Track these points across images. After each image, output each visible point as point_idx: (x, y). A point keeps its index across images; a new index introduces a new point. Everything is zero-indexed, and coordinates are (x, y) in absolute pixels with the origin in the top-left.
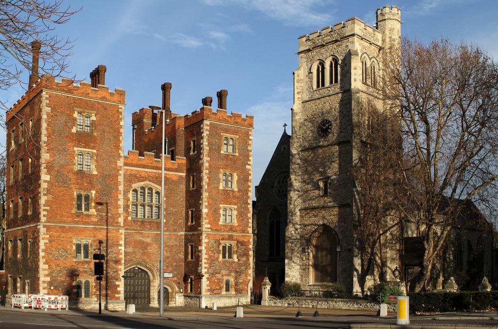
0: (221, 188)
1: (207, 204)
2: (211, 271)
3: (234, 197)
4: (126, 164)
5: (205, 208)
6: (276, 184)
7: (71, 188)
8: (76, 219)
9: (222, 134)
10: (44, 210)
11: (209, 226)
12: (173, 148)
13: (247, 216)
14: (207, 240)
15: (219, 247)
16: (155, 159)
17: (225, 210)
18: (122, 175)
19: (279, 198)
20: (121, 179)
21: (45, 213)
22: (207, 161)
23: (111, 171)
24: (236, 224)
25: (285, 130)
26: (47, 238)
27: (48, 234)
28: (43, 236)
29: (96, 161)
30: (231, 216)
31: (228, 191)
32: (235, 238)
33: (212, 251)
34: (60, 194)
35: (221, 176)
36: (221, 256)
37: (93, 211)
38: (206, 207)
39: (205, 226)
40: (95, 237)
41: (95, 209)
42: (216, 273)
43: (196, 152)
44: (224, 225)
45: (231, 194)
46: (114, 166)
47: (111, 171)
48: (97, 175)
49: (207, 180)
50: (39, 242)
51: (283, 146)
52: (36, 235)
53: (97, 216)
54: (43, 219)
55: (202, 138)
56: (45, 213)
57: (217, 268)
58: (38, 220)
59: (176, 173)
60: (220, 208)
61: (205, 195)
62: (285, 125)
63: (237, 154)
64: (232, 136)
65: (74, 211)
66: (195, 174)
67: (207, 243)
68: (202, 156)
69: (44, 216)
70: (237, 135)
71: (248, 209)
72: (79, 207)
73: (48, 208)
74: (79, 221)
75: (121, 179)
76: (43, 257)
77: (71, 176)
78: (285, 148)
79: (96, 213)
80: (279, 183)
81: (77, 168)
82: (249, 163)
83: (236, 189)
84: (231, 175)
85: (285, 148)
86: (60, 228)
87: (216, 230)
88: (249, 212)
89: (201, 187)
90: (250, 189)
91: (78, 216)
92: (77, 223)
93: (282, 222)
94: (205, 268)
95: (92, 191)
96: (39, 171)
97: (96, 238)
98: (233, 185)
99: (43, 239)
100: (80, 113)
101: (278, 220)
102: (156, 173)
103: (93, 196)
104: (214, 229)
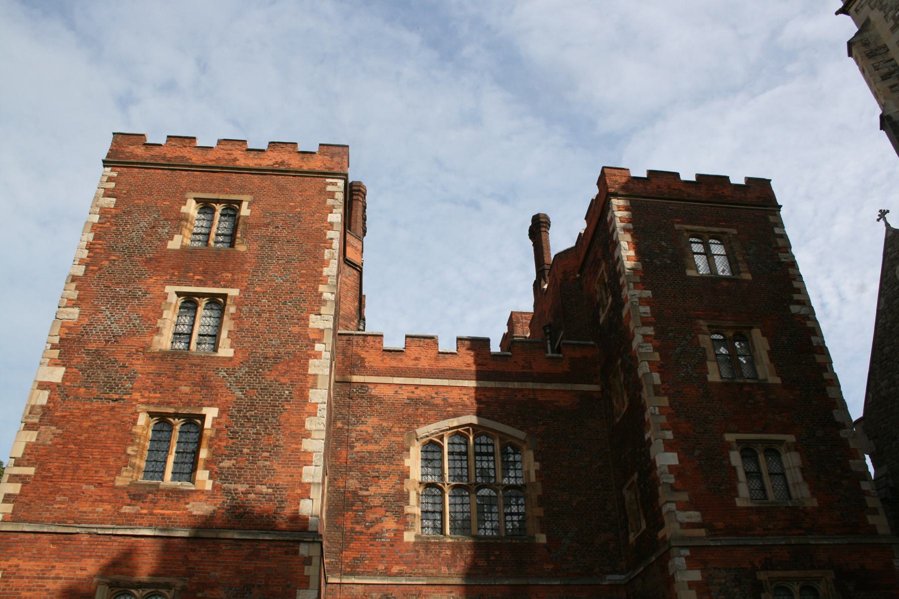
0: (713, 377)
1: (669, 435)
5: (666, 450)
7: (131, 403)
8: (126, 509)
9: (677, 226)
14: (696, 575)
17: (748, 451)
22: (643, 301)
23: (284, 344)
24: (814, 503)
25: (887, 225)
30: (783, 475)
34: (86, 424)
37: (202, 475)
38: (669, 446)
39: (679, 518)
41: (206, 468)
46: (296, 329)
47: (284, 344)
48: (230, 359)
49: (657, 357)
53: (211, 495)
56: (15, 488)
59: (569, 387)
60: (728, 447)
61: (655, 407)
62: (883, 214)
72: (156, 468)
73: (31, 471)
74: (138, 515)
77: (138, 365)
79: (209, 486)
81: (164, 341)
82: (796, 297)
83: (778, 380)
86: (53, 542)
92: (130, 520)
95: (205, 411)
97: (195, 579)
98: (758, 368)
102: (498, 390)
103: (208, 424)
104: (720, 525)
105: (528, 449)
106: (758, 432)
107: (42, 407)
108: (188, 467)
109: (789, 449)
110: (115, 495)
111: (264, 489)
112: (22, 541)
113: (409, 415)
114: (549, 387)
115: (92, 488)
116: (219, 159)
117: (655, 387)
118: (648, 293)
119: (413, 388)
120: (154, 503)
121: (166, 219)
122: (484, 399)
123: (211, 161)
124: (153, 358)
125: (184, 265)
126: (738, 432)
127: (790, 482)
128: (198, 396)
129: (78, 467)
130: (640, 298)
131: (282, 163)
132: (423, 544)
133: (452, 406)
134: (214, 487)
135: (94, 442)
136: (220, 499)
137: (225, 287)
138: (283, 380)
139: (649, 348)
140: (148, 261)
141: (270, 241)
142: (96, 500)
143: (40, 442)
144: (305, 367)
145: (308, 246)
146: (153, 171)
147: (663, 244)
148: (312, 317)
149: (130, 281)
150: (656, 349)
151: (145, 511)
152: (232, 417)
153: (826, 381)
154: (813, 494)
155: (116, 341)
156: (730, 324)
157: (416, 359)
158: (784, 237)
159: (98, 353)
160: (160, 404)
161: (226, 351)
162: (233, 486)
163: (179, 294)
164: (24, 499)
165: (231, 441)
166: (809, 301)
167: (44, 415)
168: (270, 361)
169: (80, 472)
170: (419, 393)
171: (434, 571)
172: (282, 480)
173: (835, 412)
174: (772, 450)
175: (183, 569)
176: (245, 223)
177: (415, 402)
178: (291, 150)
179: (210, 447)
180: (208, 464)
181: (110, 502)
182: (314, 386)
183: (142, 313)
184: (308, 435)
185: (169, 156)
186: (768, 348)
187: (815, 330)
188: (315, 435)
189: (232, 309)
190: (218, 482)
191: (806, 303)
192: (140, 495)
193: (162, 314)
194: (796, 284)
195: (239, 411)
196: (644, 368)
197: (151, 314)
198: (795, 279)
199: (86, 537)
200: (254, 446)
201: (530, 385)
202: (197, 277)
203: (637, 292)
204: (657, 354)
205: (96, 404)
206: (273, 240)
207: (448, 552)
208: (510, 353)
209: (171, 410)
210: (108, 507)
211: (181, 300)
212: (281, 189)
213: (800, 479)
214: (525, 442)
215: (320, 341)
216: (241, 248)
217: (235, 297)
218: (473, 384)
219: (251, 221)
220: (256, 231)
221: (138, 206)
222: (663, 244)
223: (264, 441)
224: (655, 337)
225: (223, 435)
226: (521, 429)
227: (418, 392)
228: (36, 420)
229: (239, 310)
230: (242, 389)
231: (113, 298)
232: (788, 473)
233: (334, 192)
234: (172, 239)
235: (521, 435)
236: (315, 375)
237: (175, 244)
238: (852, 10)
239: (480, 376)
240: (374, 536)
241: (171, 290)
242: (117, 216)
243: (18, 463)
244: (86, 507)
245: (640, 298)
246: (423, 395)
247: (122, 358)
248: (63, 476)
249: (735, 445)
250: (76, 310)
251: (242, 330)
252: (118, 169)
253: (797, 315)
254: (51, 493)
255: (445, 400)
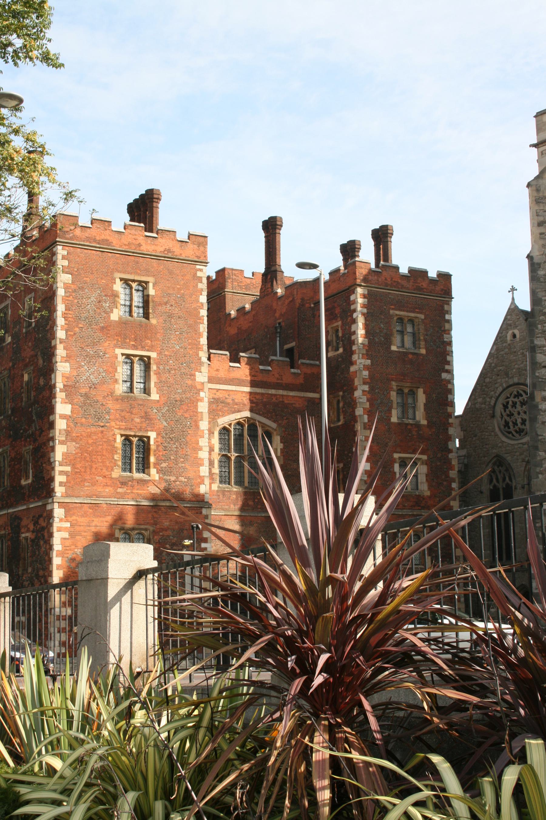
0: (394, 419)
4: (211, 380)
6: (499, 408)
8: (120, 490)
9: (391, 312)
10: (61, 473)
12: (293, 344)
13: (447, 476)
16: (261, 367)
17: (403, 463)
18: (206, 400)
19: (507, 437)
20: (203, 407)
21: (63, 478)
22: (366, 367)
24: (428, 493)
25: (513, 299)
26: (66, 528)
27: (67, 521)
28: (59, 525)
29: (157, 373)
31: (409, 427)
34: (90, 441)
35: (393, 394)
37: (153, 471)
40: (156, 525)
41: (155, 468)
43: (341, 350)
45: (414, 433)
46: (189, 382)
47: (184, 392)
48: (158, 401)
49: (367, 405)
50: (51, 535)
51: (510, 332)
52: (44, 524)
54: (59, 491)
55: (354, 321)
56: (63, 478)
58: (50, 493)
59: (302, 394)
60: (394, 461)
62: (513, 289)
63: (423, 351)
64: (412, 315)
65: (117, 473)
66: (341, 393)
68: (355, 357)
69: (61, 484)
70: (421, 313)
71: (449, 461)
73: (68, 469)
74: (125, 493)
75: (203, 407)
76: (59, 567)
77: (111, 405)
78: (514, 336)
79: (157, 477)
80: (505, 407)
82: (447, 367)
83: (424, 422)
84: (413, 393)
85: (514, 336)
86: (90, 508)
88: (452, 468)
89: (354, 419)
90: (451, 421)
91: (123, 484)
92: (122, 496)
93: (516, 488)
96: (52, 396)
97: (158, 526)
98: (417, 413)
99: (60, 529)
100: (126, 282)
101: (507, 485)
102: (262, 394)
103: (152, 442)
105: (277, 435)
106: (410, 453)
107: (65, 430)
108: (144, 466)
109: (422, 464)
110: (113, 483)
111: (183, 479)
112: (76, 508)
113: (213, 410)
114: (292, 394)
115: (101, 478)
116: (129, 244)
117: (365, 424)
118: (368, 362)
119: (215, 391)
120: (132, 486)
121: (106, 296)
122: (255, 400)
123: (125, 245)
124: (117, 400)
125: (123, 332)
126: (400, 453)
127: (419, 481)
128: (144, 425)
129: (91, 467)
130: (364, 365)
131: (169, 251)
133: (237, 404)
134: (160, 478)
135: (97, 452)
136: (163, 485)
137: (148, 351)
138: (187, 415)
139: (364, 399)
140: (102, 328)
141: (169, 316)
142: (104, 485)
143: (69, 452)
144: (196, 407)
145: (190, 322)
146: (90, 251)
147: (382, 325)
148: (197, 373)
149: (94, 344)
150: (368, 400)
151: (129, 491)
152: (163, 437)
153: (449, 424)
154: (429, 489)
155: (95, 388)
156: (408, 384)
157: (217, 370)
158: (449, 322)
159: (86, 396)
160: (126, 429)
161: (155, 396)
162: (168, 478)
163: (123, 355)
164: (69, 485)
165: (165, 452)
166: (453, 370)
167: (67, 435)
168: (178, 403)
169: (93, 470)
170: (219, 395)
171: (227, 507)
172: (191, 474)
173: (449, 443)
175: (152, 521)
176: (153, 301)
178: (172, 237)
179: (155, 455)
180: (155, 464)
181: (111, 486)
182: (202, 420)
183: (105, 368)
184: (201, 449)
185: (98, 238)
186: (424, 401)
187: (451, 392)
188: (204, 449)
189: (154, 367)
190: (161, 476)
191: (450, 372)
192: (125, 483)
193: (116, 369)
194: (448, 358)
195: (166, 434)
196: (359, 411)
197: (111, 369)
198: (448, 355)
199: (105, 505)
200: (176, 455)
201: (281, 392)
202: (133, 343)
203: (363, 361)
204: (368, 403)
205: (93, 429)
206: (171, 316)
207: (234, 496)
208: (270, 368)
209: (132, 433)
210: (111, 489)
211: (124, 357)
212: (171, 273)
213: (425, 480)
214: (275, 430)
215: (202, 390)
216: (153, 321)
217: (155, 359)
218: (247, 389)
219: (156, 299)
220: (160, 308)
221: (86, 283)
222: (382, 325)
223: (180, 453)
224: (369, 392)
225: (160, 448)
226: (274, 422)
227: (218, 394)
228: (64, 439)
229: (158, 367)
230: (166, 421)
231: (87, 356)
232: (419, 476)
233: (201, 277)
234: (112, 311)
235: (274, 425)
236: (202, 413)
237: (115, 316)
238: (542, 149)
239: (253, 384)
241: (119, 351)
242: (75, 291)
243: (61, 465)
244: (100, 489)
245: (364, 365)
246: (221, 396)
247: (100, 398)
248: (85, 472)
249: (397, 460)
250: (67, 364)
251: (161, 382)
252: (67, 248)
253: (445, 380)
254: (81, 481)
255: (233, 400)
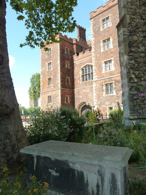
0: (102, 50)
2: (99, 103)
3: (112, 53)
11: (97, 76)
15: (103, 88)
17: (106, 63)
32: (113, 79)
33: (99, 91)
36: (104, 93)
37: (52, 85)
42: (102, 104)
44: (105, 73)
57: (103, 101)
67: (96, 87)
87: (101, 77)
92: (48, 90)
94: (95, 101)
104: (99, 77)
132: (82, 83)
174: (110, 61)
177: (80, 64)
240: (77, 83)
